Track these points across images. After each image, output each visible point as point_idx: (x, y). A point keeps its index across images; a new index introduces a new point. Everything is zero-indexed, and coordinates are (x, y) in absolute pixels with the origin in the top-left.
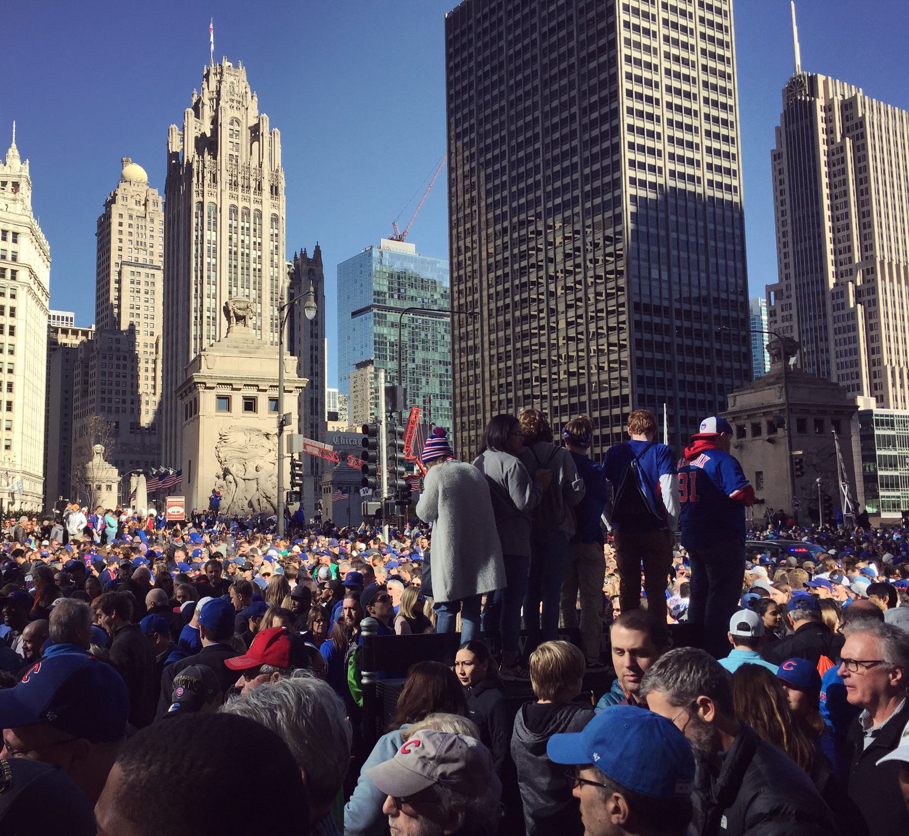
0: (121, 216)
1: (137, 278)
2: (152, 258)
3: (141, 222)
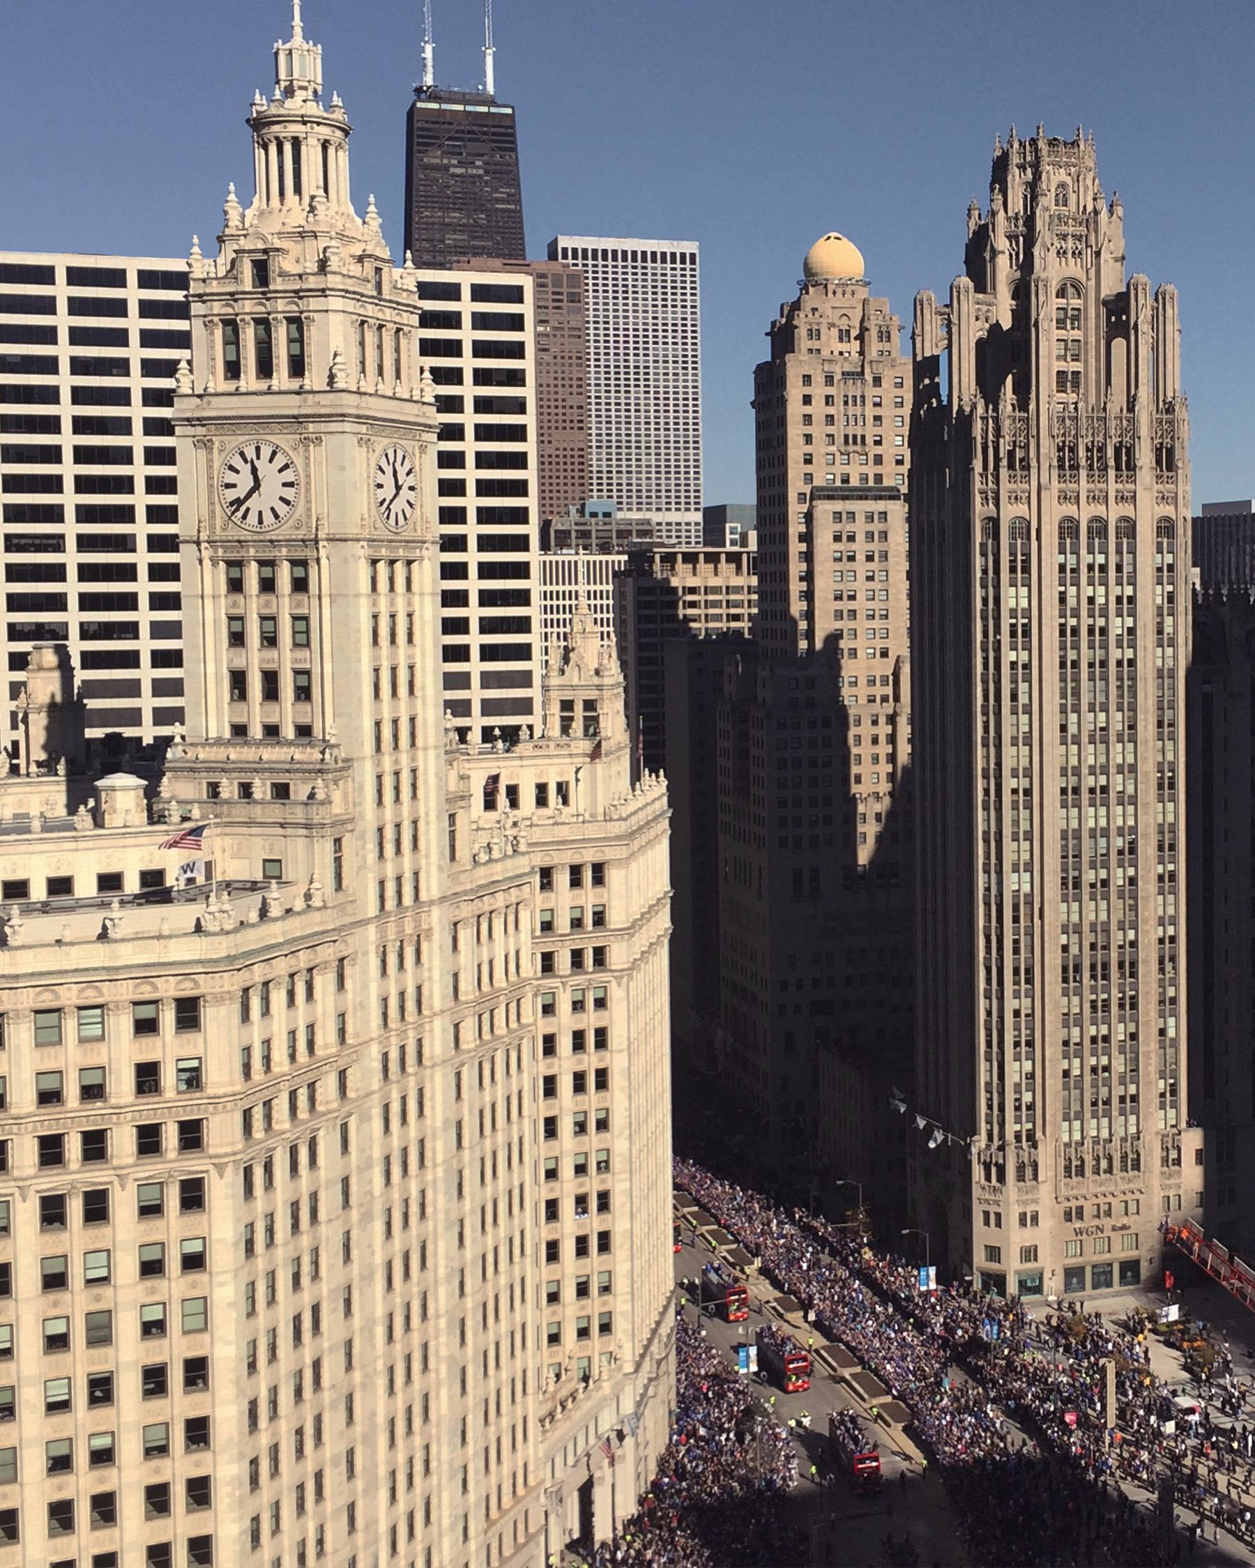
0: (807, 380)
1: (848, 527)
2: (879, 469)
3: (854, 390)
